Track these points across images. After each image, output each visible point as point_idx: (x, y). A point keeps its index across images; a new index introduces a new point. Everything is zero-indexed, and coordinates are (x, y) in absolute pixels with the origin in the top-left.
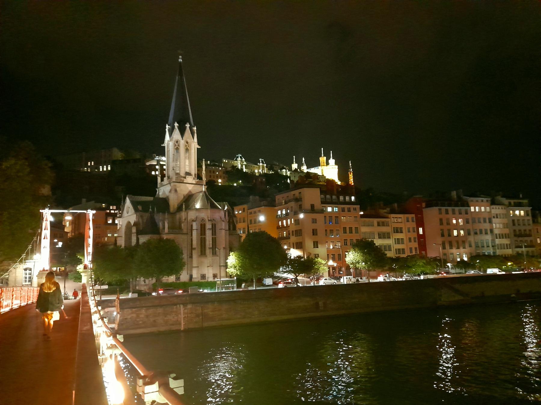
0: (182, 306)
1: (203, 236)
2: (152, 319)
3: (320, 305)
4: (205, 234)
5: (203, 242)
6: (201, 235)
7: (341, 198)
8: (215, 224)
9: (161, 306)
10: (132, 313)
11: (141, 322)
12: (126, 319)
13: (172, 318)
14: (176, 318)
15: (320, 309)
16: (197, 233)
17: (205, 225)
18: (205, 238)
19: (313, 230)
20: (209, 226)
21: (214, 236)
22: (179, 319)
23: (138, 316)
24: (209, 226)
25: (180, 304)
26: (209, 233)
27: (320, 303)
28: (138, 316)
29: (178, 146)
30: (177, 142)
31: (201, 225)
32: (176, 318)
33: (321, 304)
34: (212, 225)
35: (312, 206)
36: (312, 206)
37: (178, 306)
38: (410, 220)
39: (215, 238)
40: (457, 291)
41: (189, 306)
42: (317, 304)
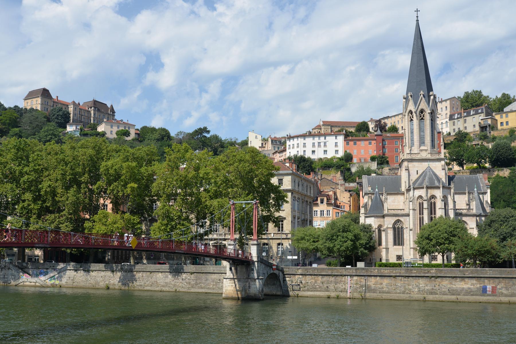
0: (349, 277)
1: (421, 216)
2: (325, 286)
3: (488, 289)
4: (423, 214)
6: (420, 214)
10: (312, 279)
11: (318, 287)
12: (307, 283)
13: (340, 286)
14: (344, 286)
15: (488, 293)
17: (423, 203)
18: (423, 218)
20: (425, 205)
22: (346, 288)
23: (316, 282)
24: (425, 205)
25: (347, 276)
26: (426, 212)
27: (488, 287)
28: (316, 282)
29: (413, 117)
31: (420, 203)
32: (344, 286)
33: (489, 288)
42: (484, 290)
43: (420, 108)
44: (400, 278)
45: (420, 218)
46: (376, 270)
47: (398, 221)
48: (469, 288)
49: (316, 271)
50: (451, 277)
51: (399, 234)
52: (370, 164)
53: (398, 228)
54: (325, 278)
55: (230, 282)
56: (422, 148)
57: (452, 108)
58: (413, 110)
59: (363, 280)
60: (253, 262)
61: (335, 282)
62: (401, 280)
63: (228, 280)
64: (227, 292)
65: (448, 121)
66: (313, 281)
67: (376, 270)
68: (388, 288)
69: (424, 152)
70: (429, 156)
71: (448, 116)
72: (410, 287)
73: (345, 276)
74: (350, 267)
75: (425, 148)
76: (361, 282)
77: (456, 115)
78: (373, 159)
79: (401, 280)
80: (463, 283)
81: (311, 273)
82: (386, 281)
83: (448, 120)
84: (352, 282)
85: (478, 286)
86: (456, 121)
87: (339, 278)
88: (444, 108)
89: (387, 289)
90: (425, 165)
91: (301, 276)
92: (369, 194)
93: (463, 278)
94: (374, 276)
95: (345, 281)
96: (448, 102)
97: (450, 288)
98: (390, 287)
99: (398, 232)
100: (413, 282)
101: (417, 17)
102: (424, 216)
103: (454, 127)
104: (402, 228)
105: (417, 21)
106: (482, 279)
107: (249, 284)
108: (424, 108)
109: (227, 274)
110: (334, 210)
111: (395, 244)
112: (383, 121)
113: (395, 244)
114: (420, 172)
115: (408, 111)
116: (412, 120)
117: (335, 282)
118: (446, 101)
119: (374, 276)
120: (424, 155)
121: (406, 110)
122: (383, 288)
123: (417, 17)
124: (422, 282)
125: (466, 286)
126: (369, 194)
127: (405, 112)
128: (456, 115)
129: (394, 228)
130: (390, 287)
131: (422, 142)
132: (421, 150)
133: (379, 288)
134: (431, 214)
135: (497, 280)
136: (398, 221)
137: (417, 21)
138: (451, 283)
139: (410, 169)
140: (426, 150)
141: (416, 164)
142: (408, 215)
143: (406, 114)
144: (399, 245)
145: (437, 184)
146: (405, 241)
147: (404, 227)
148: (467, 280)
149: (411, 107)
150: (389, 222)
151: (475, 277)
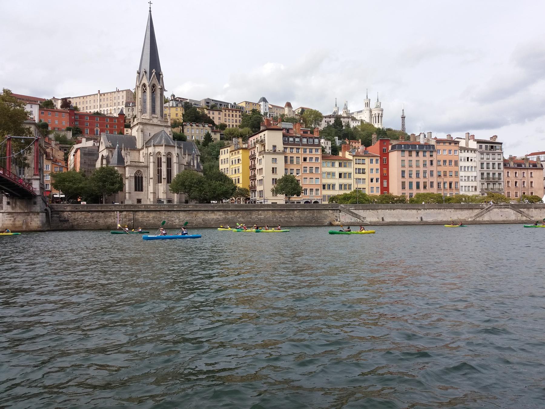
0: (118, 212)
4: (161, 166)
5: (159, 172)
6: (158, 167)
7: (305, 140)
8: (170, 159)
9: (103, 212)
10: (82, 215)
11: (87, 221)
16: (154, 165)
17: (161, 158)
19: (273, 168)
20: (164, 159)
21: (169, 168)
25: (117, 211)
28: (86, 217)
30: (145, 86)
31: (158, 158)
34: (168, 158)
35: (274, 147)
36: (274, 147)
37: (115, 212)
38: (374, 161)
39: (170, 170)
40: (356, 216)
41: (125, 213)
43: (153, 82)
44: (164, 212)
45: (158, 170)
46: (143, 206)
47: (139, 171)
48: (217, 218)
49: (86, 208)
50: (205, 210)
51: (139, 182)
52: (66, 132)
53: (139, 177)
54: (95, 214)
55: (8, 216)
56: (154, 116)
57: (127, 97)
58: (147, 84)
59: (131, 215)
60: (35, 196)
61: (105, 217)
62: (165, 214)
63: (4, 214)
64: (5, 226)
65: (124, 107)
66: (83, 216)
67: (143, 206)
68: (153, 220)
69: (155, 118)
70: (159, 123)
71: (124, 103)
72: (173, 219)
73: (114, 211)
74: (118, 204)
75: (156, 116)
76: (129, 216)
77: (131, 103)
78: (68, 129)
79: (165, 214)
80: (213, 215)
81: (81, 209)
82: (152, 215)
83: (124, 106)
84: (121, 216)
85: (224, 216)
86: (130, 108)
87: (109, 214)
88: (121, 97)
89: (153, 221)
90: (161, 129)
91: (70, 213)
92: (109, 148)
93: (213, 211)
94: (141, 211)
95: (114, 216)
96: (125, 92)
97: (203, 218)
98: (156, 220)
99: (139, 180)
100: (175, 215)
101: (150, 8)
102: (162, 168)
103: (129, 113)
104: (142, 178)
105: (150, 11)
106: (227, 211)
107: (31, 218)
108: (155, 83)
109: (4, 208)
110: (53, 165)
111: (136, 190)
112: (68, 100)
113: (136, 190)
114: (152, 135)
115: (142, 84)
116: (145, 92)
117: (105, 217)
118: (123, 91)
119: (141, 211)
120: (155, 121)
121: (141, 82)
122: (149, 220)
123: (150, 8)
124: (182, 215)
125: (215, 217)
126: (109, 148)
127: (140, 85)
128: (131, 103)
129: (135, 177)
130: (156, 220)
131: (153, 111)
132: (153, 117)
133: (146, 221)
134: (168, 166)
135: (237, 212)
136: (139, 171)
137: (150, 11)
138: (204, 215)
139: (145, 131)
140: (157, 118)
141: (149, 127)
142: (147, 167)
143: (141, 86)
144: (139, 191)
145: (172, 144)
146: (144, 188)
147: (144, 176)
148: (216, 212)
149: (145, 81)
150: (129, 173)
151: (221, 210)
